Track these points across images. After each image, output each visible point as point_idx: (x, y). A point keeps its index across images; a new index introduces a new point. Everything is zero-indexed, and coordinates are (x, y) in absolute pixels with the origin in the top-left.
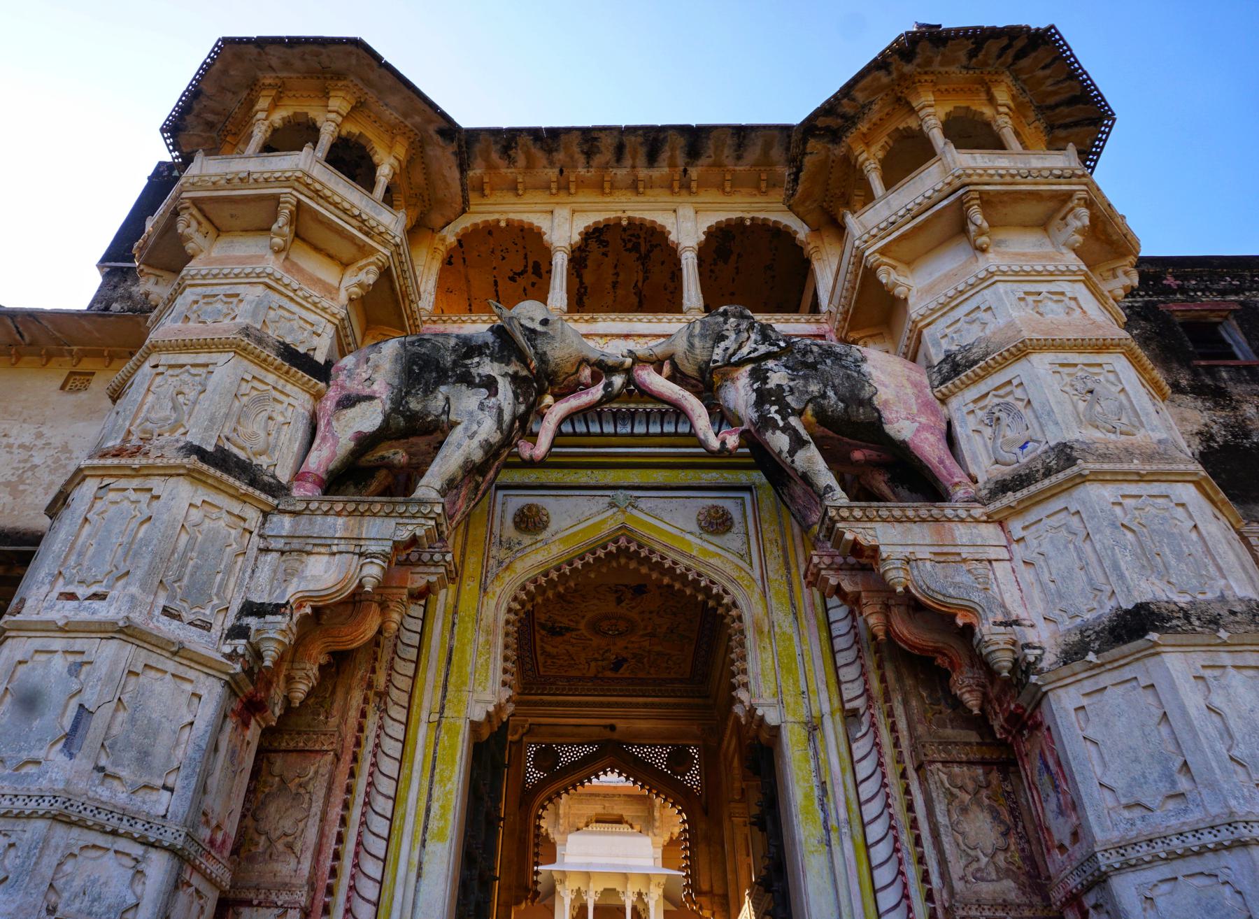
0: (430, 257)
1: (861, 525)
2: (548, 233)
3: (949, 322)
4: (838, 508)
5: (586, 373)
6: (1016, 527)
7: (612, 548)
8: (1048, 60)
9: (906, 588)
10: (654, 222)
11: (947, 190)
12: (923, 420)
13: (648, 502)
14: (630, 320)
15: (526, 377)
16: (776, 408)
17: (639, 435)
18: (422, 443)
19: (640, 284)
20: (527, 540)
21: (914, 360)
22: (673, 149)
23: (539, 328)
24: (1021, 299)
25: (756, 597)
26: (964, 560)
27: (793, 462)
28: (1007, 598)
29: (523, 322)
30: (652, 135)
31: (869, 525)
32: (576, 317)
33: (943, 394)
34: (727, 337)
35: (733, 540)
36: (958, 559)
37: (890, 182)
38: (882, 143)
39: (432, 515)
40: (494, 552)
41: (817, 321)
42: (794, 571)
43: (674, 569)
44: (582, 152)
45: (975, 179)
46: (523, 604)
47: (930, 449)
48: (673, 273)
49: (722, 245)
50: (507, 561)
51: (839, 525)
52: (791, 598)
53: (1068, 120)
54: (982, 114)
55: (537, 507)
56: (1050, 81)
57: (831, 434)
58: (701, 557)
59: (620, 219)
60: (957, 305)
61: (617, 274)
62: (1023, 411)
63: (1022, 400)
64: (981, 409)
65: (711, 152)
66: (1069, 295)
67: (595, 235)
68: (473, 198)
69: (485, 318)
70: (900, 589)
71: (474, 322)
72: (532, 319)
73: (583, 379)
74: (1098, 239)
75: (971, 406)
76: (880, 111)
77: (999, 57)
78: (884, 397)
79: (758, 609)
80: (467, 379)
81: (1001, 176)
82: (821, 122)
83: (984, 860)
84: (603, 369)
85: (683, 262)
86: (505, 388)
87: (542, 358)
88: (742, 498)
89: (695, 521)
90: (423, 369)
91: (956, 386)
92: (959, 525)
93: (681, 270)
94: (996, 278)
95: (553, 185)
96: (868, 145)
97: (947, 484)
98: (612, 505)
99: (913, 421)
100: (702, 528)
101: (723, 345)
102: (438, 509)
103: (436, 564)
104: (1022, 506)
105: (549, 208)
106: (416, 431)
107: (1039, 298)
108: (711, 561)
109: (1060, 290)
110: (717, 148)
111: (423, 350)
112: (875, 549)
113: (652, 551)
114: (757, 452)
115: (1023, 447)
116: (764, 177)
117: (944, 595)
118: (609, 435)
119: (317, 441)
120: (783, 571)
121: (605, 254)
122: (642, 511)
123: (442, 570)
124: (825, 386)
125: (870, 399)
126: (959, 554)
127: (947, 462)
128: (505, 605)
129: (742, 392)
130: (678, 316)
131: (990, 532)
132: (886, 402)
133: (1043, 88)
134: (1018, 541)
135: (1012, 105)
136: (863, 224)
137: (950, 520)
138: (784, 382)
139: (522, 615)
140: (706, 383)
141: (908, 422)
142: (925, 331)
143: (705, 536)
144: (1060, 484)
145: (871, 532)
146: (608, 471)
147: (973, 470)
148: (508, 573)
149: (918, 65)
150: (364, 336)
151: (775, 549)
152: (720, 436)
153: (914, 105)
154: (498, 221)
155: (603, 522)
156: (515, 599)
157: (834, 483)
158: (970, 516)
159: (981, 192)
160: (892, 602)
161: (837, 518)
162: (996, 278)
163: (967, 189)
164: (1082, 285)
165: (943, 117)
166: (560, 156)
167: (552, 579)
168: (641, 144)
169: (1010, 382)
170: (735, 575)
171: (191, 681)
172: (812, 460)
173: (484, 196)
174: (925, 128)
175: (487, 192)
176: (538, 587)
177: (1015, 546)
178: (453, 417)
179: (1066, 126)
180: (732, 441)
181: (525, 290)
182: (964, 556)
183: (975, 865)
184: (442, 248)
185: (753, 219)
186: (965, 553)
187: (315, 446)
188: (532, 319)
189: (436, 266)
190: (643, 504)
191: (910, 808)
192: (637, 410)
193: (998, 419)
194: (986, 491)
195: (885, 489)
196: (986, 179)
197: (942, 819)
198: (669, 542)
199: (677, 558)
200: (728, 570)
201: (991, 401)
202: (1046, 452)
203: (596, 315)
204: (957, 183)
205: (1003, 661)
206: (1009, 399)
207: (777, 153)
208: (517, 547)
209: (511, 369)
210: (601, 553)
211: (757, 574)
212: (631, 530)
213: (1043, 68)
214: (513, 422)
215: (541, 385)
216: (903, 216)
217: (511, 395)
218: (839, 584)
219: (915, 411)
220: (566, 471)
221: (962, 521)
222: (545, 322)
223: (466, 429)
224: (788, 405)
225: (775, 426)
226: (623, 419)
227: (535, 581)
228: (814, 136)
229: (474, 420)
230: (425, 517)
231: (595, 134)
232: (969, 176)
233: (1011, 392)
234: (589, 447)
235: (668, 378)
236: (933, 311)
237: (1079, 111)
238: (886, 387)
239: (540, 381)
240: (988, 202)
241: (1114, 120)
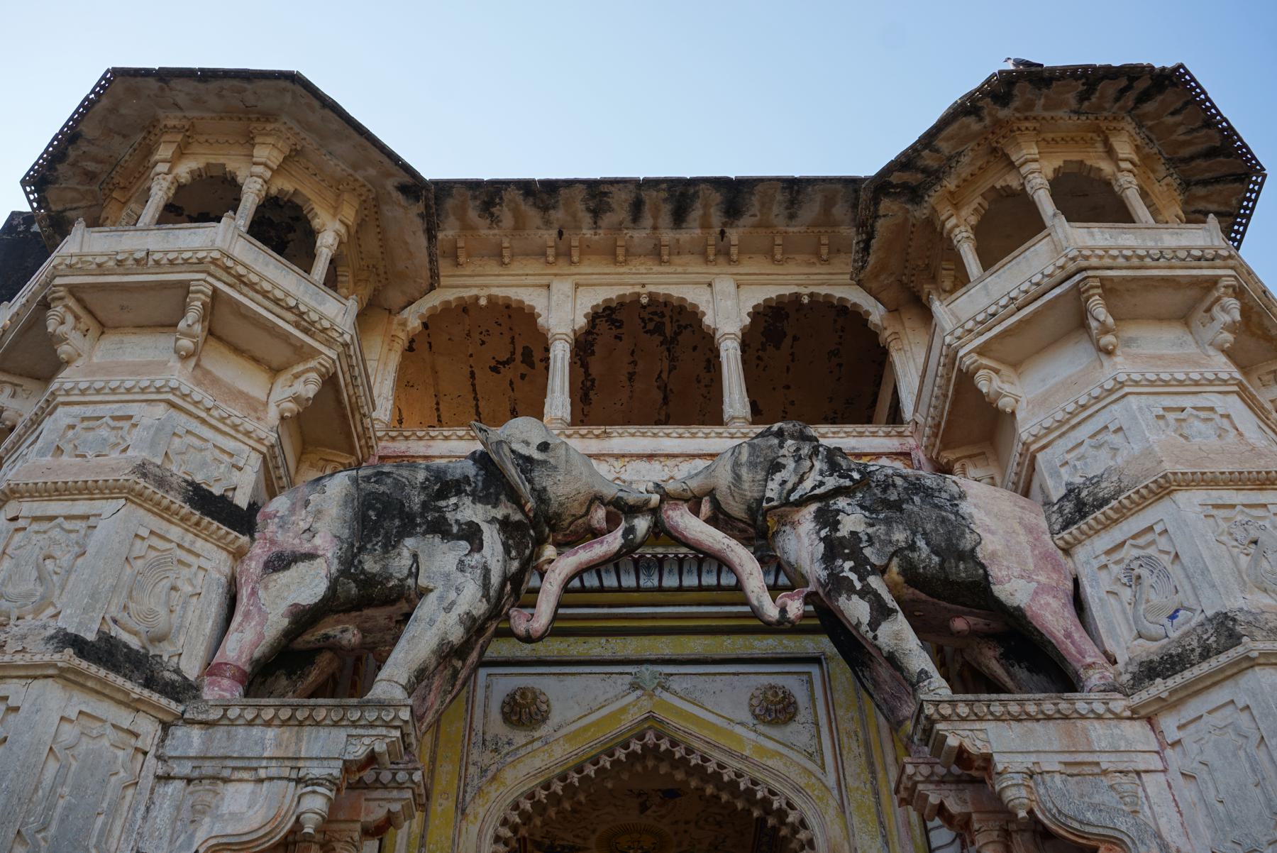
0: (386, 347)
1: (967, 725)
2: (544, 314)
3: (1070, 446)
4: (937, 703)
5: (599, 515)
6: (1169, 724)
7: (636, 746)
8: (1179, 105)
9: (1031, 812)
10: (683, 299)
11: (1059, 275)
12: (1042, 578)
13: (684, 681)
14: (655, 435)
15: (519, 523)
16: (851, 564)
17: (670, 590)
18: (380, 615)
19: (664, 375)
20: (520, 737)
21: (1026, 494)
22: (706, 206)
23: (537, 455)
24: (1159, 417)
25: (831, 813)
26: (1105, 773)
27: (875, 637)
28: (1163, 822)
29: (515, 446)
30: (678, 190)
31: (978, 725)
32: (584, 431)
33: (1067, 543)
34: (784, 466)
35: (798, 732)
36: (1096, 770)
37: (989, 260)
38: (974, 205)
39: (397, 723)
40: (475, 755)
41: (900, 435)
42: (880, 775)
43: (721, 775)
44: (588, 210)
45: (1094, 262)
46: (515, 829)
47: (1053, 618)
48: (708, 361)
49: (771, 326)
50: (494, 768)
51: (939, 726)
52: (879, 814)
53: (1207, 175)
54: (1100, 170)
55: (533, 691)
56: (1182, 129)
57: (923, 596)
58: (756, 758)
59: (639, 295)
60: (1079, 423)
61: (634, 363)
62: (1170, 568)
63: (1168, 553)
64: (1116, 563)
65: (756, 209)
66: (1220, 411)
67: (606, 316)
68: (444, 267)
69: (461, 433)
70: (1022, 814)
71: (446, 438)
72: (528, 444)
73: (595, 523)
74: (1253, 334)
75: (1104, 559)
76: (971, 164)
77: (1117, 100)
78: (990, 548)
79: (836, 830)
80: (440, 528)
81: (1127, 258)
82: (895, 178)
84: (621, 509)
85: (723, 354)
86: (492, 538)
87: (541, 496)
88: (809, 673)
89: (747, 708)
90: (384, 515)
91: (1082, 533)
92: (1096, 723)
93: (720, 364)
94: (1127, 390)
95: (551, 252)
96: (957, 206)
97: (1078, 666)
98: (634, 687)
99: (1030, 579)
100: (756, 717)
101: (778, 477)
102: (405, 715)
103: (400, 787)
104: (1174, 698)
105: (544, 280)
106: (371, 601)
107: (1183, 416)
108: (770, 763)
109: (1209, 404)
110: (763, 205)
111: (382, 489)
112: (988, 759)
113: (690, 751)
114: (825, 617)
115: (1172, 617)
116: (824, 240)
117: (1081, 822)
118: (629, 590)
120: (866, 776)
121: (618, 337)
122: (675, 693)
123: (408, 794)
124: (914, 533)
125: (973, 550)
126: (1098, 764)
127: (1076, 636)
128: (491, 832)
129: (806, 541)
130: (719, 429)
131: (1136, 733)
132: (993, 554)
133: (1174, 137)
134: (1173, 745)
135: (1136, 159)
136: (955, 313)
137: (1083, 717)
138: (860, 528)
139: (514, 844)
140: (758, 528)
141: (1022, 582)
142: (1039, 456)
143: (761, 728)
145: (981, 735)
146: (629, 639)
147: (1110, 646)
148: (494, 786)
149: (1017, 109)
150: (299, 462)
151: (854, 745)
152: (779, 601)
153: (1014, 158)
154: (477, 298)
155: (623, 710)
156: (505, 822)
157: (930, 667)
158: (1109, 710)
159: (1102, 279)
160: (1013, 827)
161: (936, 716)
162: (1127, 390)
163: (1085, 274)
164: (1236, 397)
165: (1051, 175)
166: (558, 215)
167: (555, 793)
168: (665, 200)
169: (1151, 529)
170: (802, 782)
172: (899, 635)
173: (458, 264)
174: (1028, 189)
175: (461, 260)
176: (537, 804)
177: (1169, 752)
178: (422, 582)
179: (1205, 183)
180: (795, 607)
181: (511, 383)
182: (1104, 766)
184: (402, 335)
185: (811, 295)
186: (1106, 762)
188: (528, 444)
189: (394, 359)
190: (675, 684)
192: (665, 556)
193: (1139, 577)
194: (1128, 676)
195: (997, 669)
196: (1107, 262)
198: (711, 737)
199: (725, 759)
200: (792, 776)
201: (1129, 553)
202: (1202, 625)
203: (609, 429)
204: (1071, 267)
206: (1151, 551)
207: (840, 211)
208: (506, 749)
209: (499, 513)
210: (621, 754)
211: (831, 780)
212: (662, 721)
213: (1173, 114)
214: (503, 585)
215: (540, 533)
216: (1005, 307)
217: (500, 548)
219: (1031, 566)
220: (571, 639)
221: (1099, 717)
222: (544, 447)
223: (441, 598)
224: (866, 560)
225: (851, 590)
226: (648, 568)
227: (531, 796)
228: (888, 194)
229: (450, 584)
230: (387, 725)
231: (605, 188)
232: (1087, 258)
233: (1153, 542)
234: (603, 606)
235: (707, 521)
236: (1049, 430)
237: (1220, 165)
238: (993, 533)
240: (1110, 290)
241: (1265, 176)
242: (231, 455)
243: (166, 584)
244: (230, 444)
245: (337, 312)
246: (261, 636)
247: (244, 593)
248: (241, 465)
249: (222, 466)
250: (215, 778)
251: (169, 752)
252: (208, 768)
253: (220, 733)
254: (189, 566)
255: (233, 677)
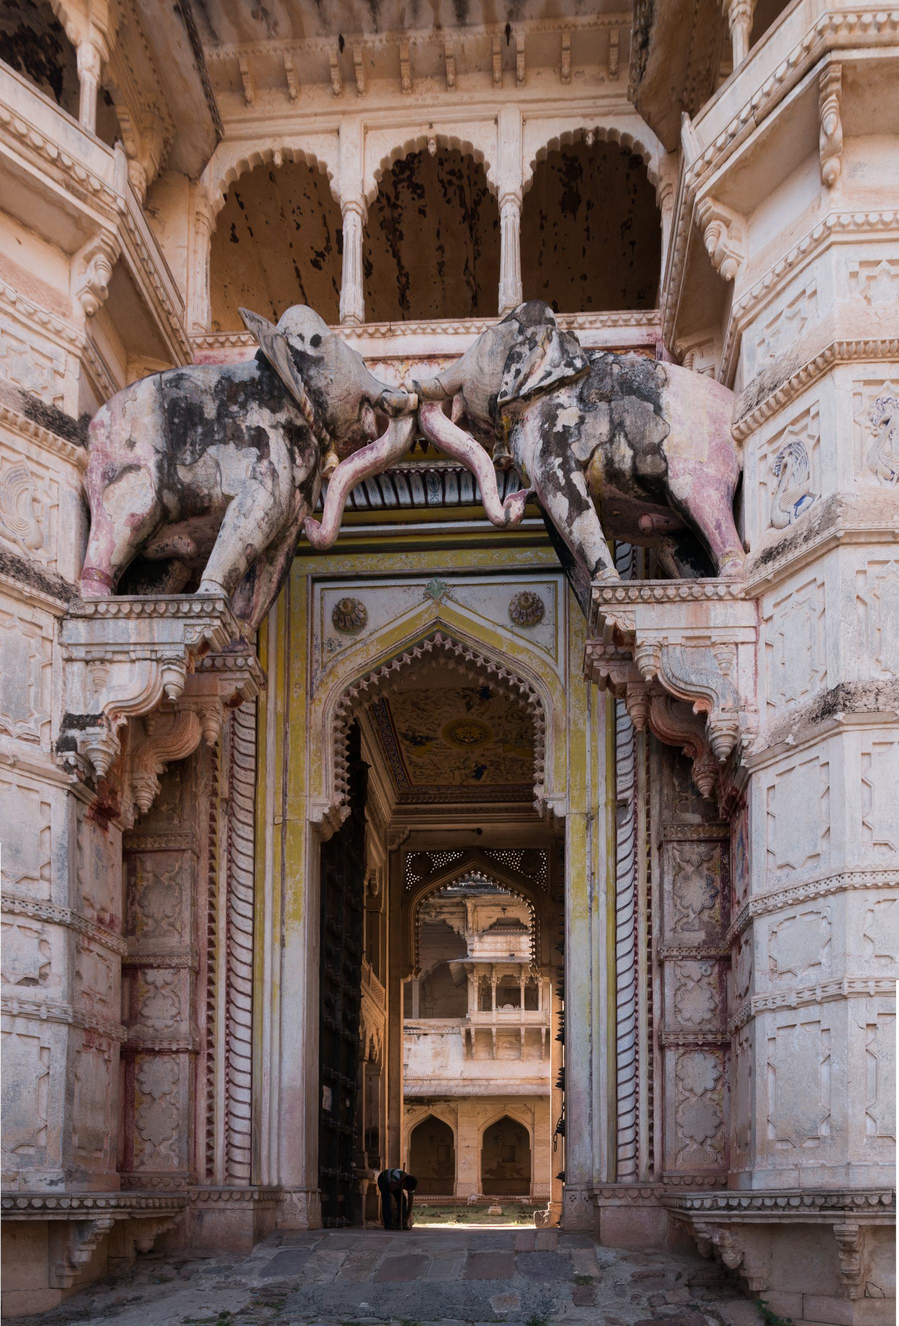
23: (311, 351)
26: (714, 644)
28: (742, 682)
36: (708, 643)
72: (301, 337)
80: (236, 437)
83: (692, 916)
87: (317, 395)
91: (756, 421)
92: (717, 604)
97: (719, 554)
103: (241, 669)
119: (93, 527)
132: (676, 446)
134: (767, 621)
137: (709, 599)
140: (492, 424)
144: (815, 551)
158: (730, 594)
171: (37, 792)
172: (588, 532)
180: (517, 507)
182: (713, 640)
183: (685, 920)
187: (92, 534)
188: (301, 337)
191: (649, 880)
197: (667, 887)
205: (723, 746)
209: (282, 417)
218: (608, 677)
219: (705, 459)
221: (721, 599)
238: (681, 424)
239: (320, 434)
242: (51, 359)
243: (26, 497)
244: (47, 347)
245: (110, 171)
246: (113, 544)
247: (93, 504)
248: (61, 370)
249: (45, 371)
250: (103, 661)
251: (65, 640)
252: (97, 653)
253: (97, 624)
254: (42, 478)
255: (100, 581)
